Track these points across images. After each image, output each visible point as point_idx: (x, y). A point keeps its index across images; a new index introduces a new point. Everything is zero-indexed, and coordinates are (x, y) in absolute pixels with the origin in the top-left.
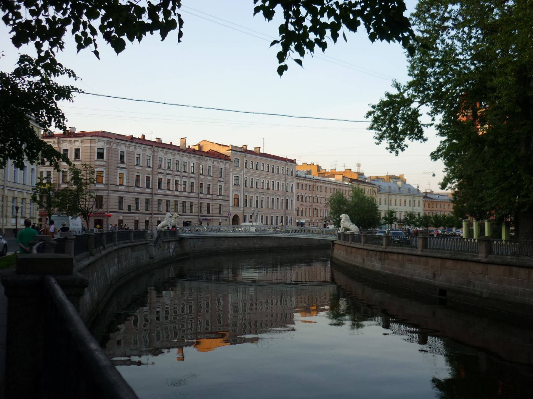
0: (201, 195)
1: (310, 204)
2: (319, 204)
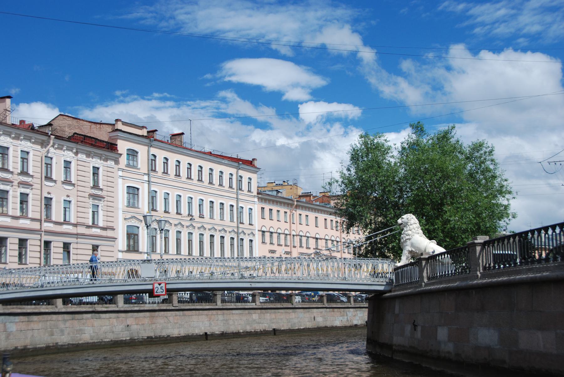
0: (47, 226)
1: (288, 249)
2: (304, 250)
